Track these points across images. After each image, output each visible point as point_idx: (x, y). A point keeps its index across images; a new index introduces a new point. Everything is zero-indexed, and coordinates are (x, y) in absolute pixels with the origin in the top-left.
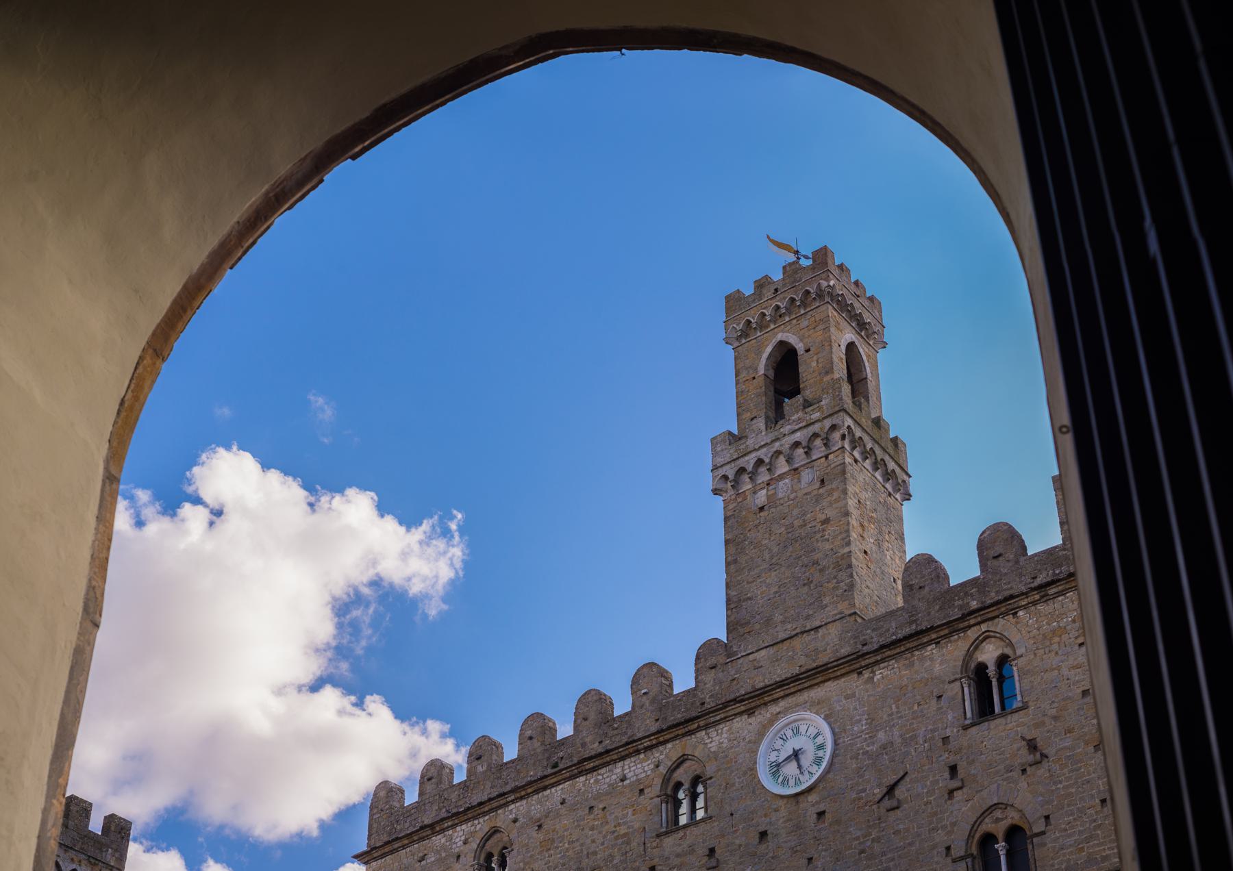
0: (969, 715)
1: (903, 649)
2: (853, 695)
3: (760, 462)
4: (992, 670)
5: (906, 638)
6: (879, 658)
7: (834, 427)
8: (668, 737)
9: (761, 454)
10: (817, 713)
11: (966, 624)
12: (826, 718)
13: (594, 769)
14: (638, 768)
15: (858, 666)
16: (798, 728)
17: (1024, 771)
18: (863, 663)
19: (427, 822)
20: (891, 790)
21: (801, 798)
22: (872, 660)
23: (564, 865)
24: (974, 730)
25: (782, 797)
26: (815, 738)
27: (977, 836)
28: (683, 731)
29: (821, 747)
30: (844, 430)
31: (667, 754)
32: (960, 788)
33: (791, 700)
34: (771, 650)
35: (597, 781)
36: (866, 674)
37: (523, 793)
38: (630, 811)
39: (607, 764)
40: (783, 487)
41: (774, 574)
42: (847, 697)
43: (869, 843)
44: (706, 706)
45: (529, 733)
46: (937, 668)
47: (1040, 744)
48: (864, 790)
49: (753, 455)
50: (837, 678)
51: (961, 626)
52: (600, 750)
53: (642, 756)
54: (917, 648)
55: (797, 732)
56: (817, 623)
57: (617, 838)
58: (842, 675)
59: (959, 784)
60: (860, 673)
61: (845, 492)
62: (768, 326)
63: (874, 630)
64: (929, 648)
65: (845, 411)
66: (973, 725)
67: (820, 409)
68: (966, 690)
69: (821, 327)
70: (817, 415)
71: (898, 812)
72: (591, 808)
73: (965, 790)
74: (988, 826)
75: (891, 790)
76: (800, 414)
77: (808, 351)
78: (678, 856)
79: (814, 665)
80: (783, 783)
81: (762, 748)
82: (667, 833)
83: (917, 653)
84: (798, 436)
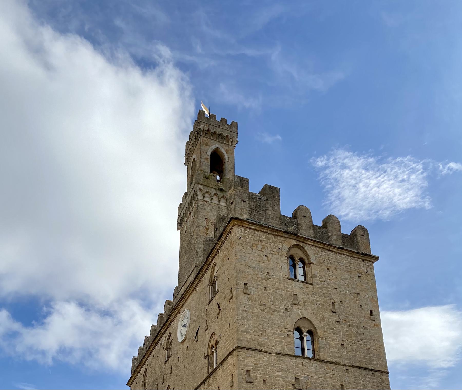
6: (196, 283)
20: (197, 333)
25: (181, 343)
32: (207, 329)
51: (209, 262)
68: (210, 288)
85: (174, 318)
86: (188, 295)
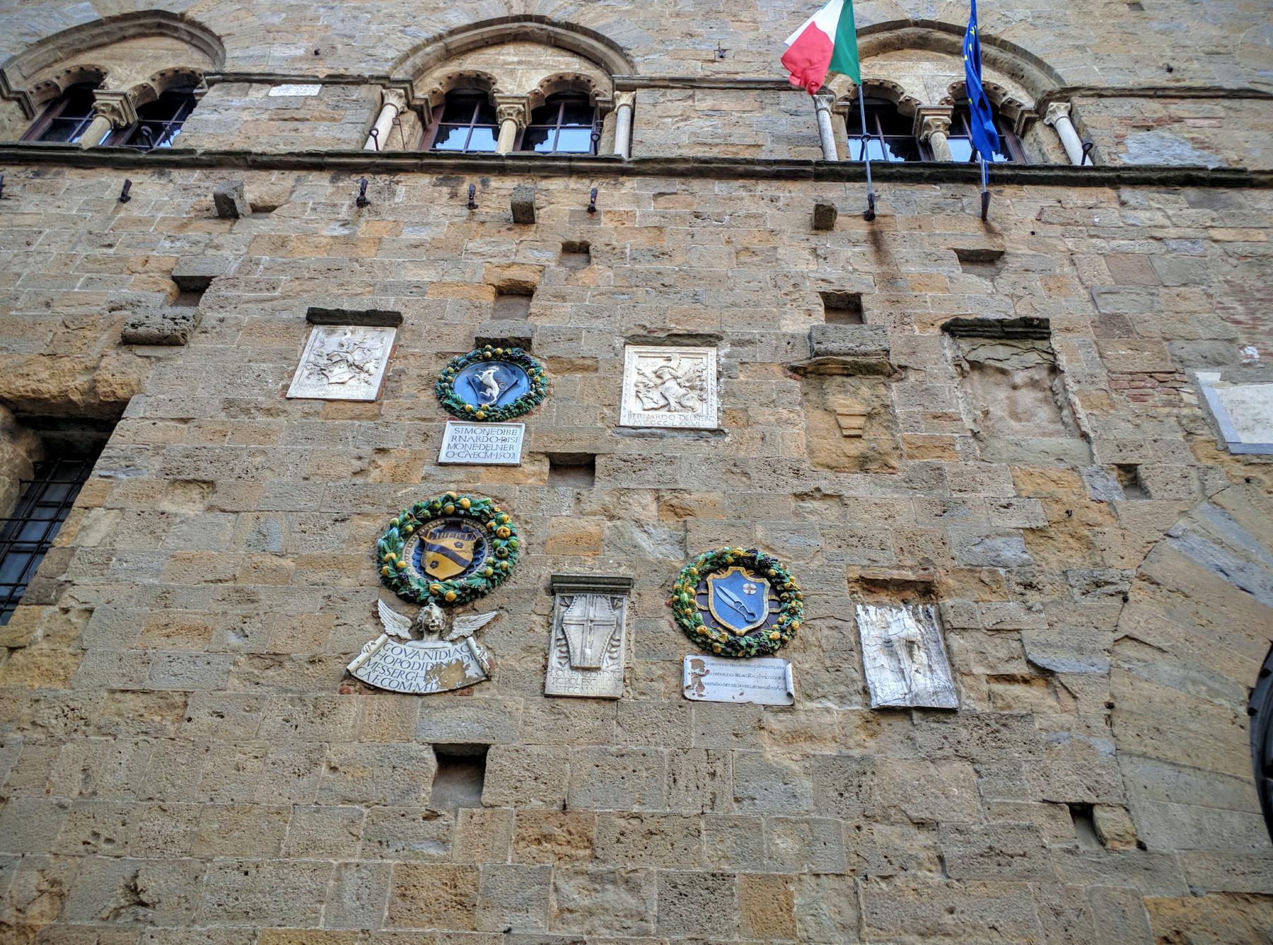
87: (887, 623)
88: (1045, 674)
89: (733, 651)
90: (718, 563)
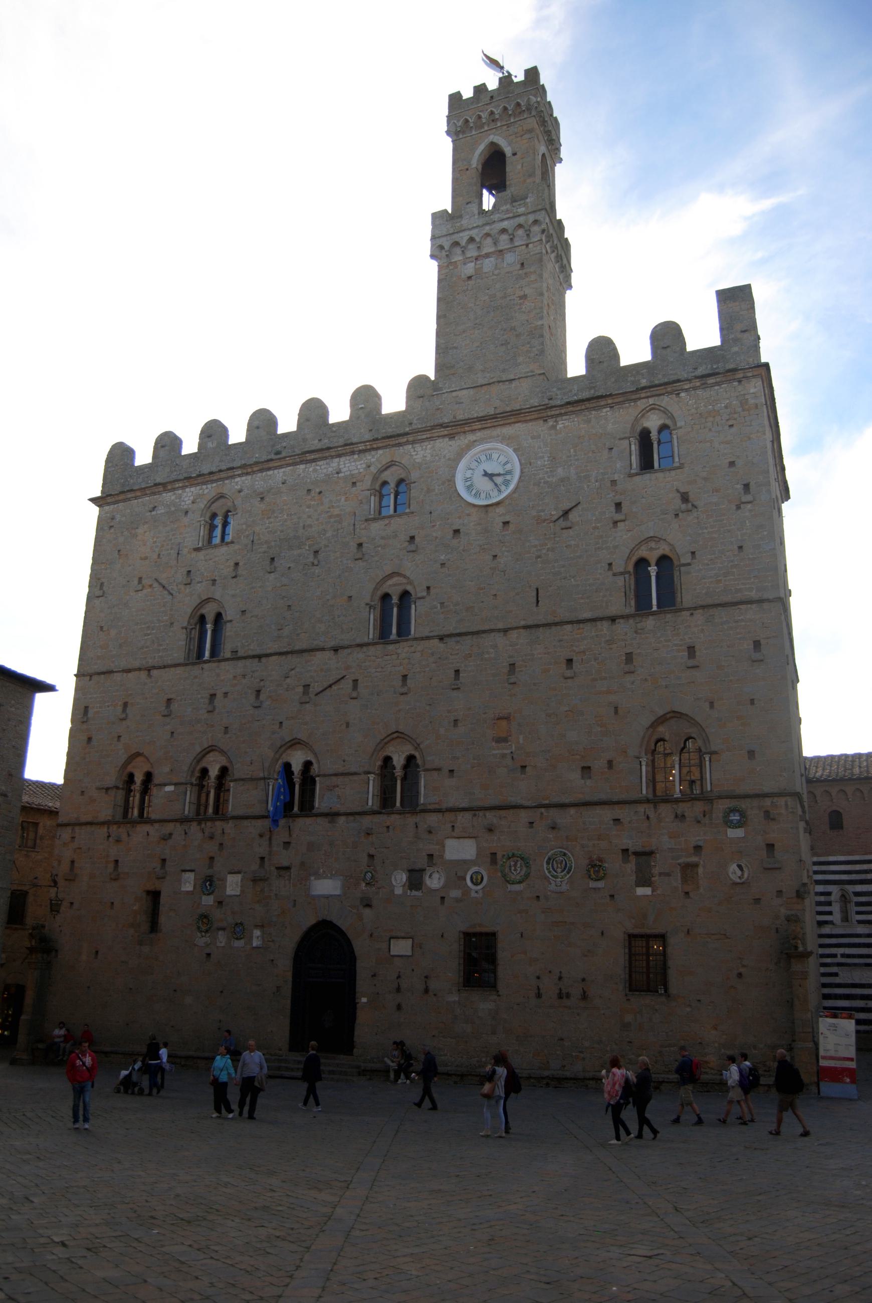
0: (634, 466)
1: (583, 407)
2: (539, 437)
3: (472, 240)
4: (654, 435)
5: (588, 400)
6: (563, 411)
7: (536, 222)
8: (381, 445)
9: (474, 233)
10: (507, 445)
11: (638, 396)
12: (515, 450)
13: (314, 460)
14: (351, 466)
15: (545, 414)
16: (491, 455)
17: (677, 515)
18: (549, 414)
19: (158, 480)
20: (566, 513)
21: (490, 509)
22: (557, 412)
23: (282, 531)
24: (637, 479)
25: (474, 506)
26: (505, 464)
27: (634, 559)
28: (394, 442)
29: (509, 472)
30: (544, 226)
31: (378, 458)
32: (624, 521)
33: (487, 432)
34: (472, 391)
35: (315, 471)
36: (551, 422)
37: (249, 470)
38: (343, 499)
39: (325, 458)
40: (488, 264)
41: (476, 332)
42: (533, 438)
43: (544, 551)
44: (414, 427)
45: (256, 423)
46: (610, 427)
47: (691, 496)
48: (543, 511)
49: (467, 233)
50: (526, 421)
51: (633, 397)
52: (319, 446)
53: (356, 456)
54: (594, 408)
55: (489, 458)
56: (512, 377)
57: (330, 517)
58: (531, 420)
59: (623, 517)
60: (546, 421)
61: (541, 276)
62: (482, 126)
63: (559, 389)
64: (604, 410)
65: (546, 210)
66: (637, 474)
67: (525, 205)
69: (527, 136)
70: (522, 210)
71: (570, 531)
72: (309, 491)
73: (627, 523)
74: (643, 552)
75: (566, 513)
76: (508, 206)
77: (514, 154)
78: (382, 538)
79: (508, 409)
80: (475, 495)
81: (462, 466)
82: (374, 519)
83: (593, 412)
84: (505, 224)
85: (423, 440)
86: (513, 420)
87: (257, 933)
88: (273, 941)
89: (237, 939)
90: (237, 924)
